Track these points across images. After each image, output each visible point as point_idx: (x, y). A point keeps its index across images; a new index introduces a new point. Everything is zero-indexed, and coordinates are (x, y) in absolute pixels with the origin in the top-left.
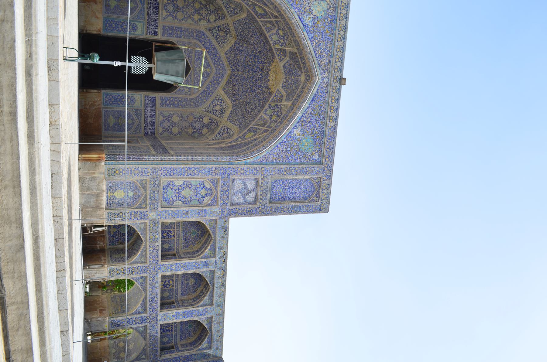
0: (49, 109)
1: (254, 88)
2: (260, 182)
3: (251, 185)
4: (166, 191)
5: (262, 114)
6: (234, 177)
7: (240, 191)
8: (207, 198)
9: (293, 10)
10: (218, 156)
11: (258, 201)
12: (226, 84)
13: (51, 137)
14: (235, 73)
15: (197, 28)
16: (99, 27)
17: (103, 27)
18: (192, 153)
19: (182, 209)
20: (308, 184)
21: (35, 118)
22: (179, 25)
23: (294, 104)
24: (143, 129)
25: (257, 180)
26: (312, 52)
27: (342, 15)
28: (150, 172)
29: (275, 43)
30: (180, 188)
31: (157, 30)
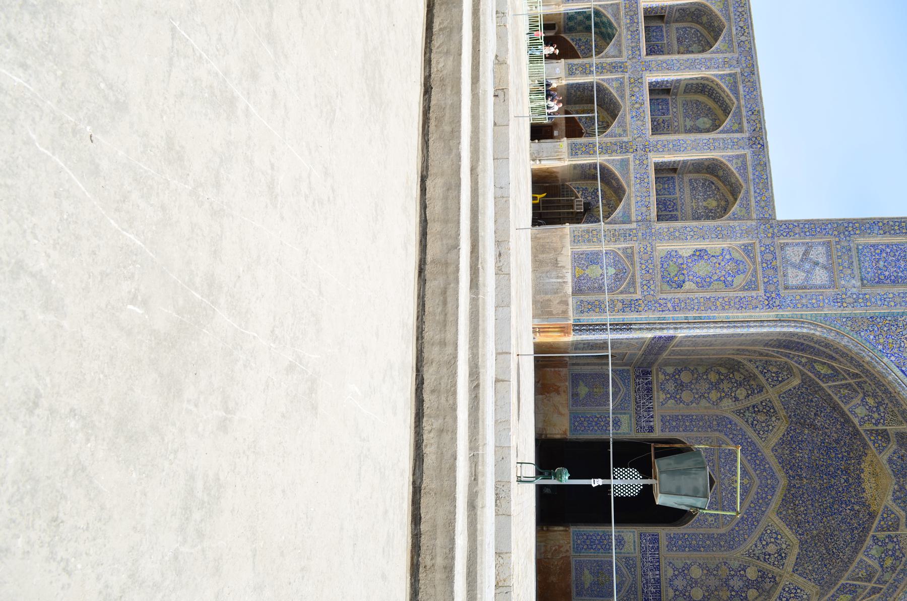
5: (861, 556)
14: (796, 482)
15: (718, 412)
16: (564, 428)
17: (570, 427)
22: (686, 412)
24: (640, 593)
31: (652, 424)
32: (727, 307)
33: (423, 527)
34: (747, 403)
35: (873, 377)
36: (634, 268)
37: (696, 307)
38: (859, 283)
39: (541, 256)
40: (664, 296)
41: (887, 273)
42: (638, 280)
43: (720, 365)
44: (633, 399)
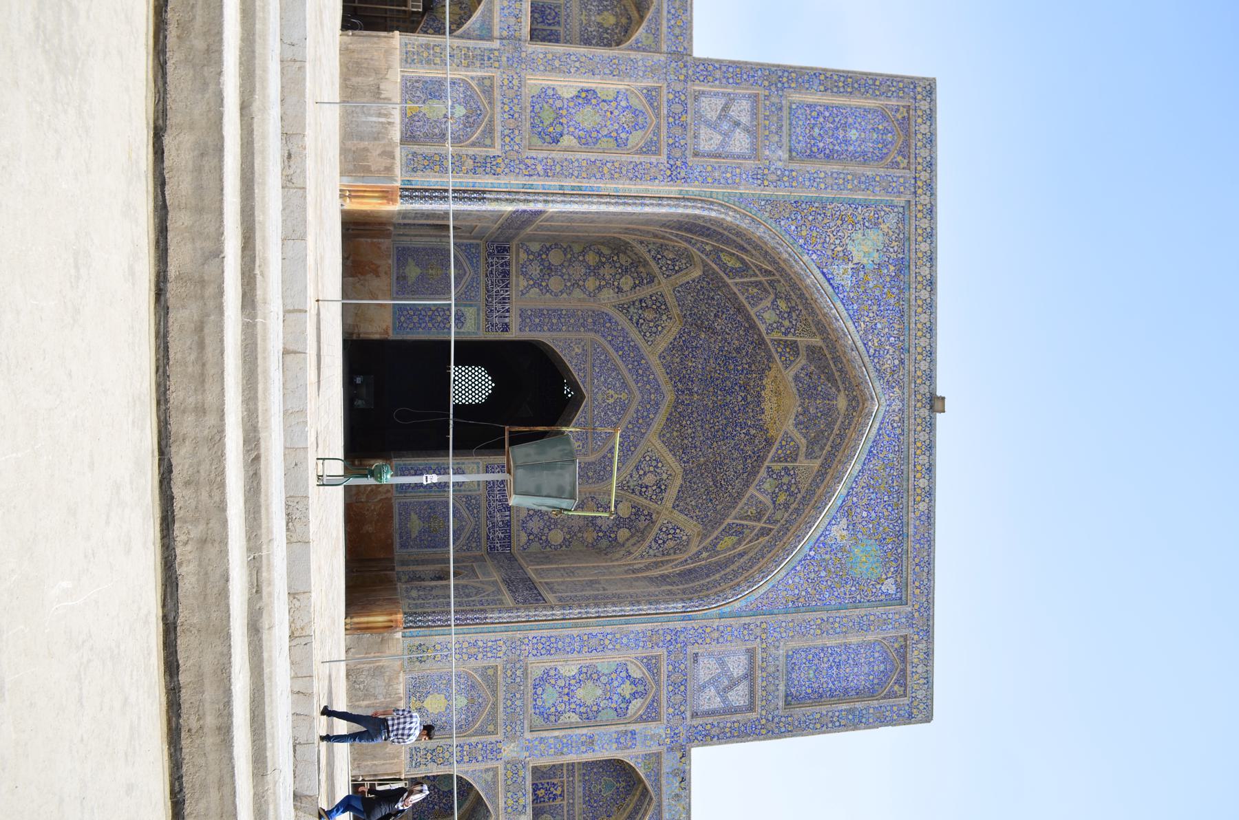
0: (290, 602)
1: (729, 429)
2: (759, 657)
3: (737, 666)
4: (539, 691)
5: (752, 490)
6: (696, 649)
7: (714, 681)
8: (636, 704)
9: (805, 258)
10: (657, 602)
11: (758, 703)
12: (666, 425)
13: (292, 663)
14: (685, 397)
15: (595, 306)
17: (394, 324)
18: (596, 597)
19: (577, 731)
20: (877, 655)
21: (267, 719)
22: (554, 305)
23: (826, 466)
24: (484, 540)
25: (751, 653)
26: (859, 344)
27: (920, 255)
28: (504, 648)
29: (770, 329)
30: (573, 682)
31: (507, 320)
32: (616, 175)
33: (183, 678)
34: (634, 296)
35: (789, 279)
36: (492, 109)
37: (576, 173)
38: (786, 156)
39: (355, 80)
40: (533, 154)
41: (821, 145)
42: (498, 128)
43: (602, 244)
44: (482, 285)
